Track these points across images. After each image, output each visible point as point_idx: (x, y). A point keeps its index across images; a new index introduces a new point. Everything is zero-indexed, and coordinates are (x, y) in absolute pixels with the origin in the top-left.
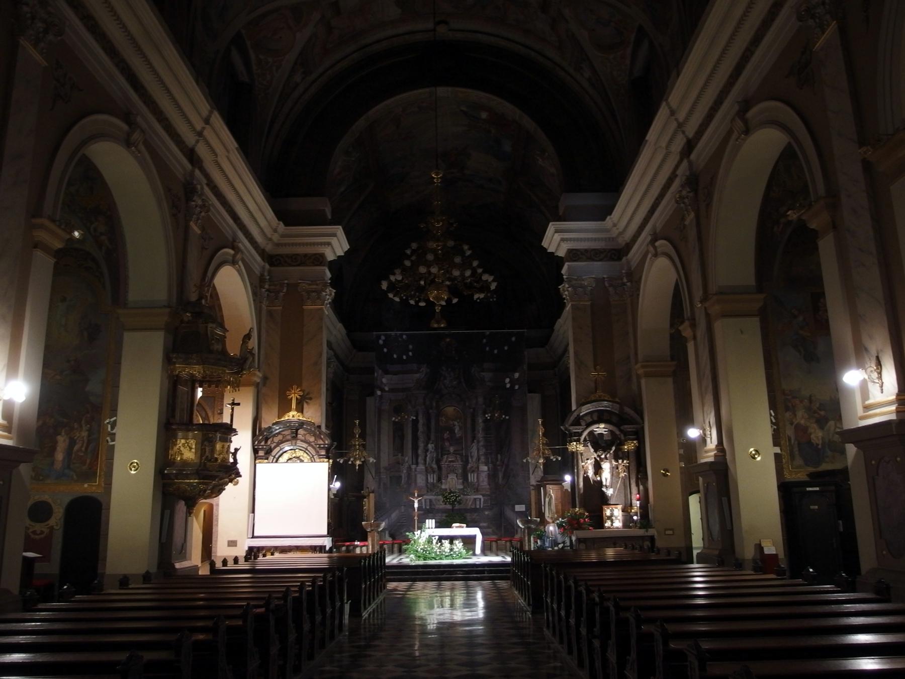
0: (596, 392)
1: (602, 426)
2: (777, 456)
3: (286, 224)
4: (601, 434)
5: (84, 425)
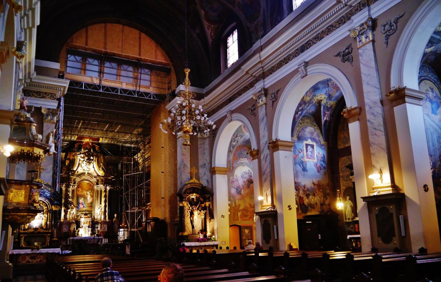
1: (195, 194)
3: (37, 74)
4: (193, 199)
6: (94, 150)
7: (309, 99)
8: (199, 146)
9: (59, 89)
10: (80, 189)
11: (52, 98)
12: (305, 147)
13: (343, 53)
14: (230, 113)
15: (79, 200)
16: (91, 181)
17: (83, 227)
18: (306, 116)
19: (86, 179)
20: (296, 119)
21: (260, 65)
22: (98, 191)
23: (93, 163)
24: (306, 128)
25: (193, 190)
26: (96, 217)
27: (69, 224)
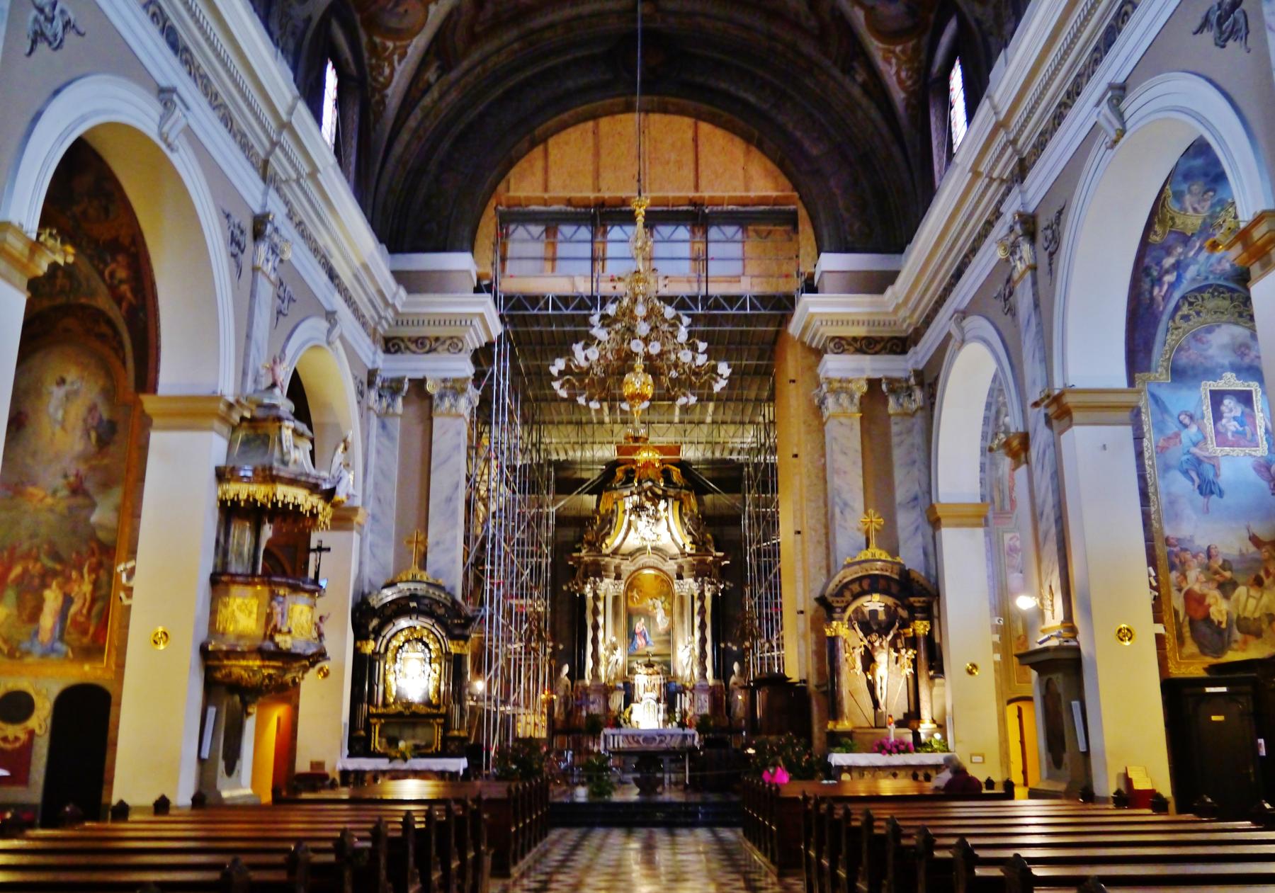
0: (867, 547)
1: (876, 597)
2: (1160, 639)
3: (410, 291)
5: (86, 576)
6: (668, 480)
7: (1200, 222)
8: (895, 440)
9: (469, 323)
11: (452, 350)
12: (1208, 401)
13: (1218, 13)
14: (956, 319)
16: (665, 568)
18: (1211, 286)
19: (652, 564)
20: (1158, 307)
21: (1002, 138)
22: (682, 598)
23: (667, 519)
24: (1210, 330)
25: (873, 584)
26: (680, 673)
27: (606, 691)
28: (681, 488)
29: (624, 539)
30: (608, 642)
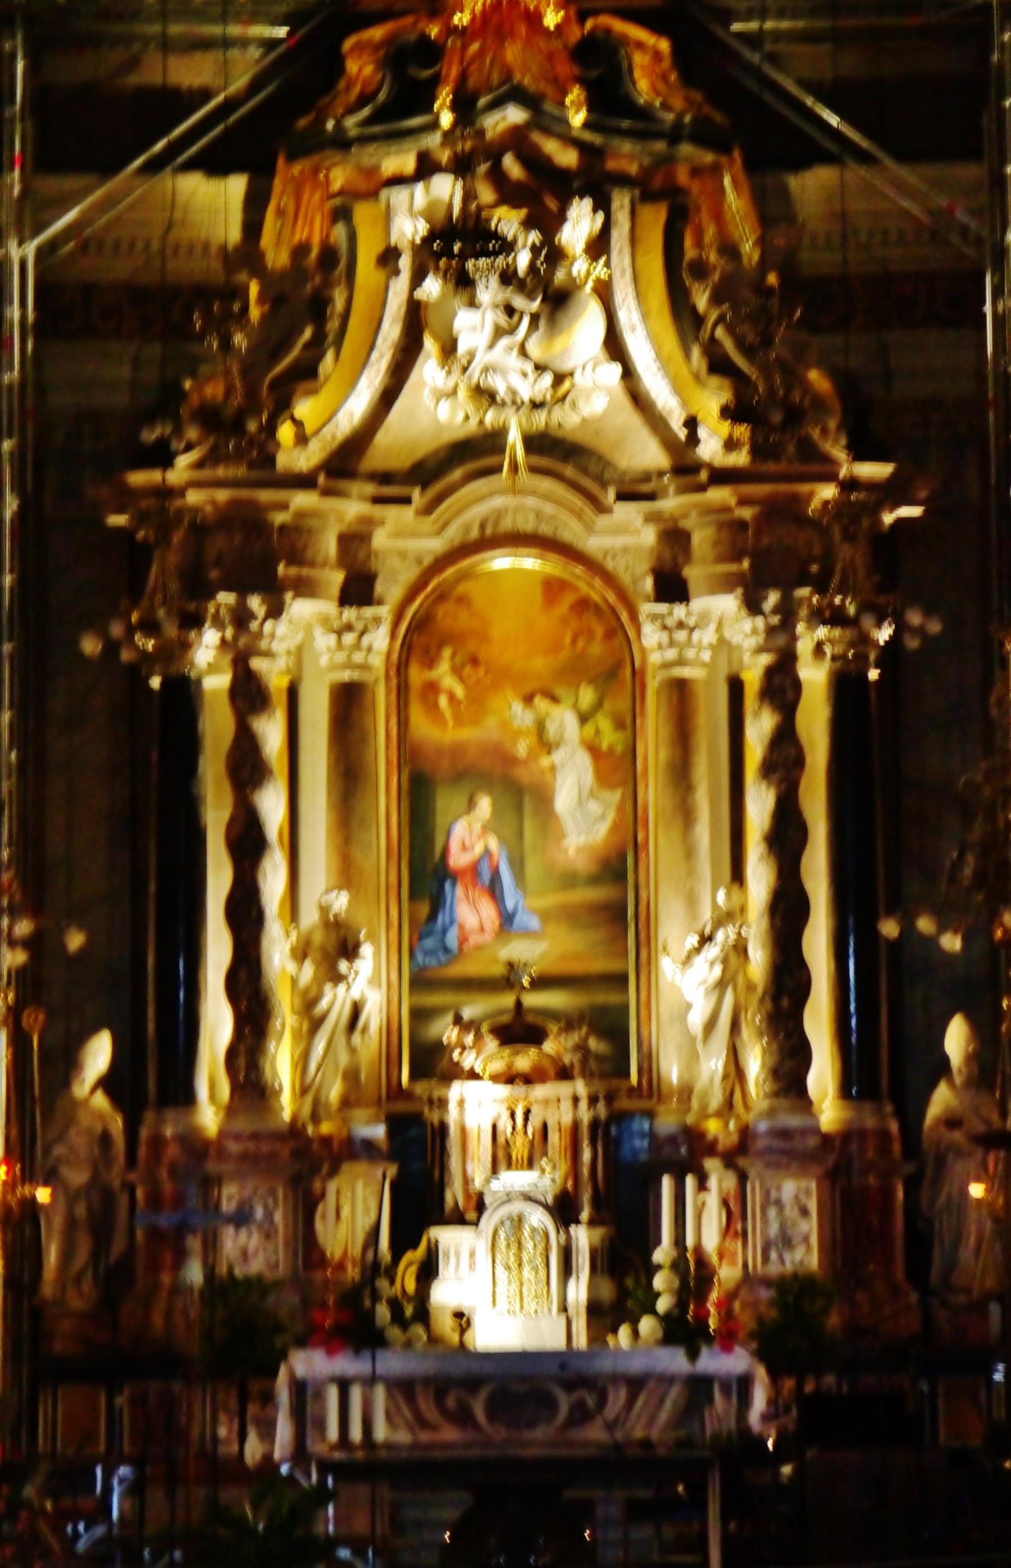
10: (443, 673)
15: (441, 820)
16: (594, 544)
17: (480, 1207)
19: (527, 524)
23: (604, 292)
28: (675, 135)
29: (388, 397)
30: (310, 917)
